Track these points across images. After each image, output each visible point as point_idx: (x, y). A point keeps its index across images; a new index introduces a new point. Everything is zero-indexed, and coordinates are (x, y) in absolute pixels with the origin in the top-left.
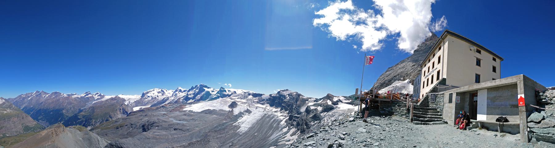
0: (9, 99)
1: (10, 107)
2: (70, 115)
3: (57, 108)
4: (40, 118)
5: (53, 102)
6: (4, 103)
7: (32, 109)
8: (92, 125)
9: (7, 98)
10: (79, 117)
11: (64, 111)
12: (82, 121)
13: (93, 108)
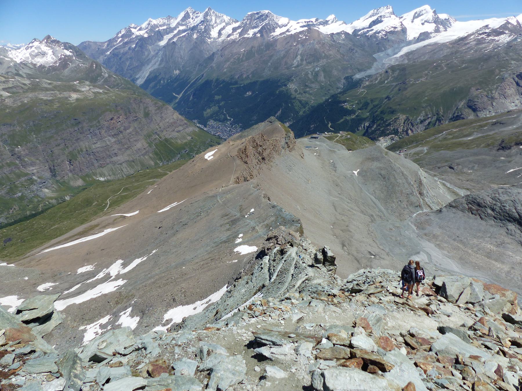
0: (85, 46)
1: (92, 76)
2: (314, 98)
3: (267, 74)
4: (208, 112)
5: (249, 54)
6: (64, 62)
7: (180, 83)
8: (396, 132)
9: (76, 43)
10: (347, 106)
11: (292, 86)
12: (359, 121)
13: (402, 72)
